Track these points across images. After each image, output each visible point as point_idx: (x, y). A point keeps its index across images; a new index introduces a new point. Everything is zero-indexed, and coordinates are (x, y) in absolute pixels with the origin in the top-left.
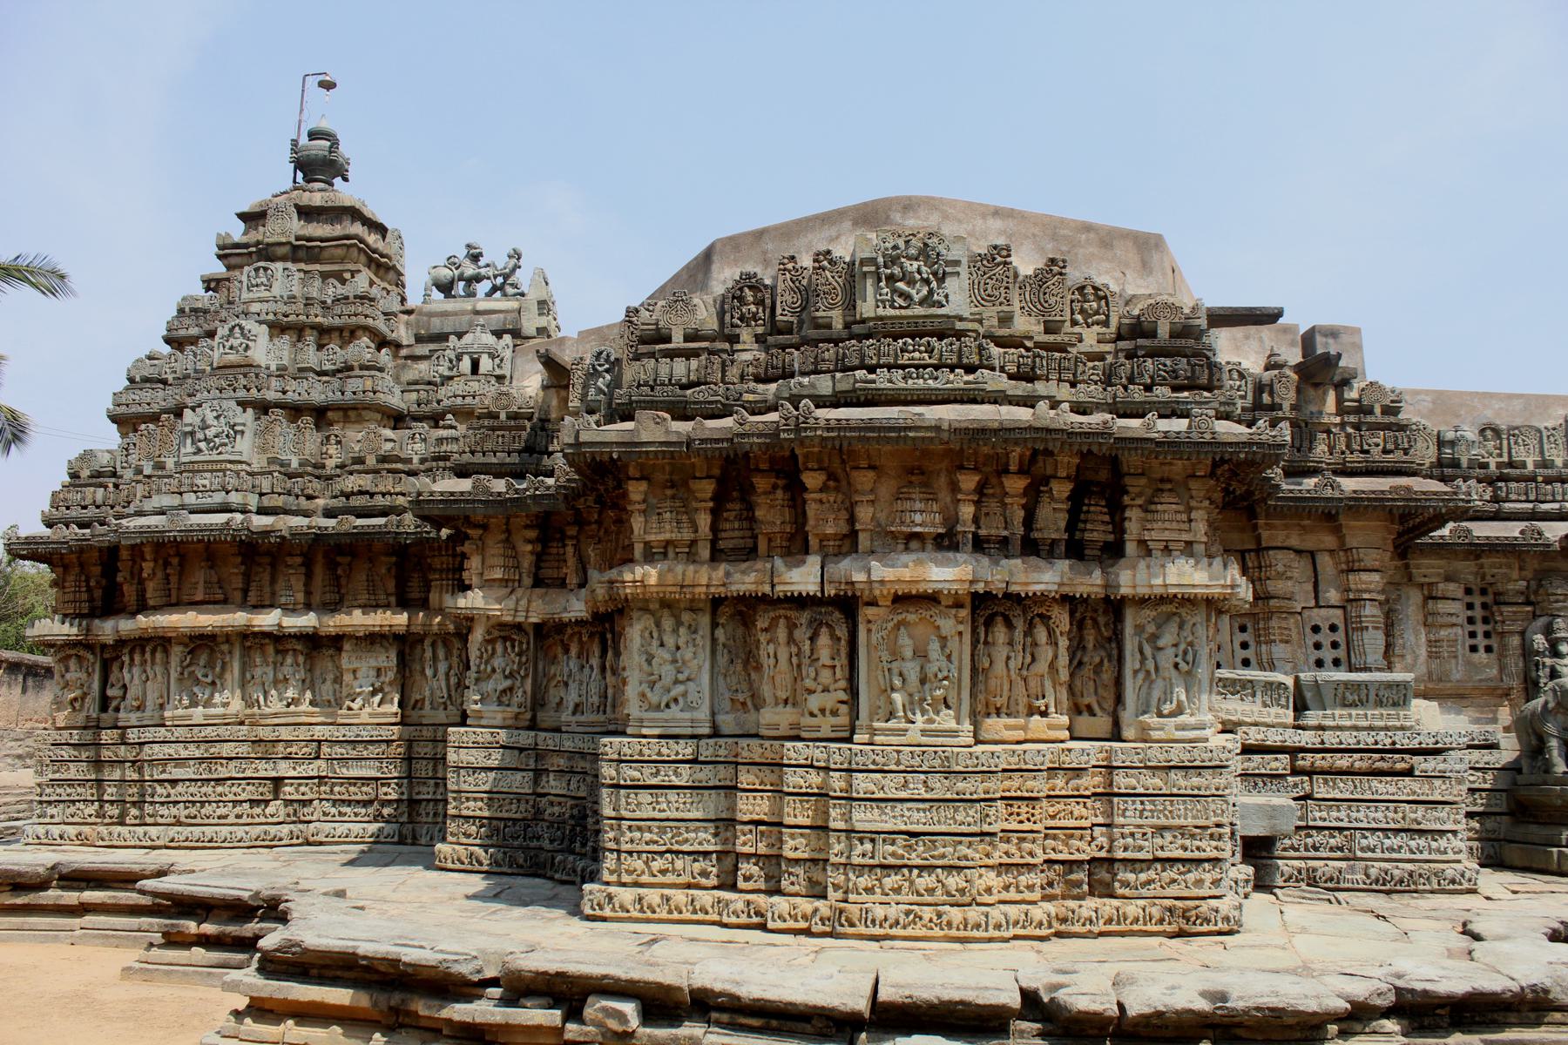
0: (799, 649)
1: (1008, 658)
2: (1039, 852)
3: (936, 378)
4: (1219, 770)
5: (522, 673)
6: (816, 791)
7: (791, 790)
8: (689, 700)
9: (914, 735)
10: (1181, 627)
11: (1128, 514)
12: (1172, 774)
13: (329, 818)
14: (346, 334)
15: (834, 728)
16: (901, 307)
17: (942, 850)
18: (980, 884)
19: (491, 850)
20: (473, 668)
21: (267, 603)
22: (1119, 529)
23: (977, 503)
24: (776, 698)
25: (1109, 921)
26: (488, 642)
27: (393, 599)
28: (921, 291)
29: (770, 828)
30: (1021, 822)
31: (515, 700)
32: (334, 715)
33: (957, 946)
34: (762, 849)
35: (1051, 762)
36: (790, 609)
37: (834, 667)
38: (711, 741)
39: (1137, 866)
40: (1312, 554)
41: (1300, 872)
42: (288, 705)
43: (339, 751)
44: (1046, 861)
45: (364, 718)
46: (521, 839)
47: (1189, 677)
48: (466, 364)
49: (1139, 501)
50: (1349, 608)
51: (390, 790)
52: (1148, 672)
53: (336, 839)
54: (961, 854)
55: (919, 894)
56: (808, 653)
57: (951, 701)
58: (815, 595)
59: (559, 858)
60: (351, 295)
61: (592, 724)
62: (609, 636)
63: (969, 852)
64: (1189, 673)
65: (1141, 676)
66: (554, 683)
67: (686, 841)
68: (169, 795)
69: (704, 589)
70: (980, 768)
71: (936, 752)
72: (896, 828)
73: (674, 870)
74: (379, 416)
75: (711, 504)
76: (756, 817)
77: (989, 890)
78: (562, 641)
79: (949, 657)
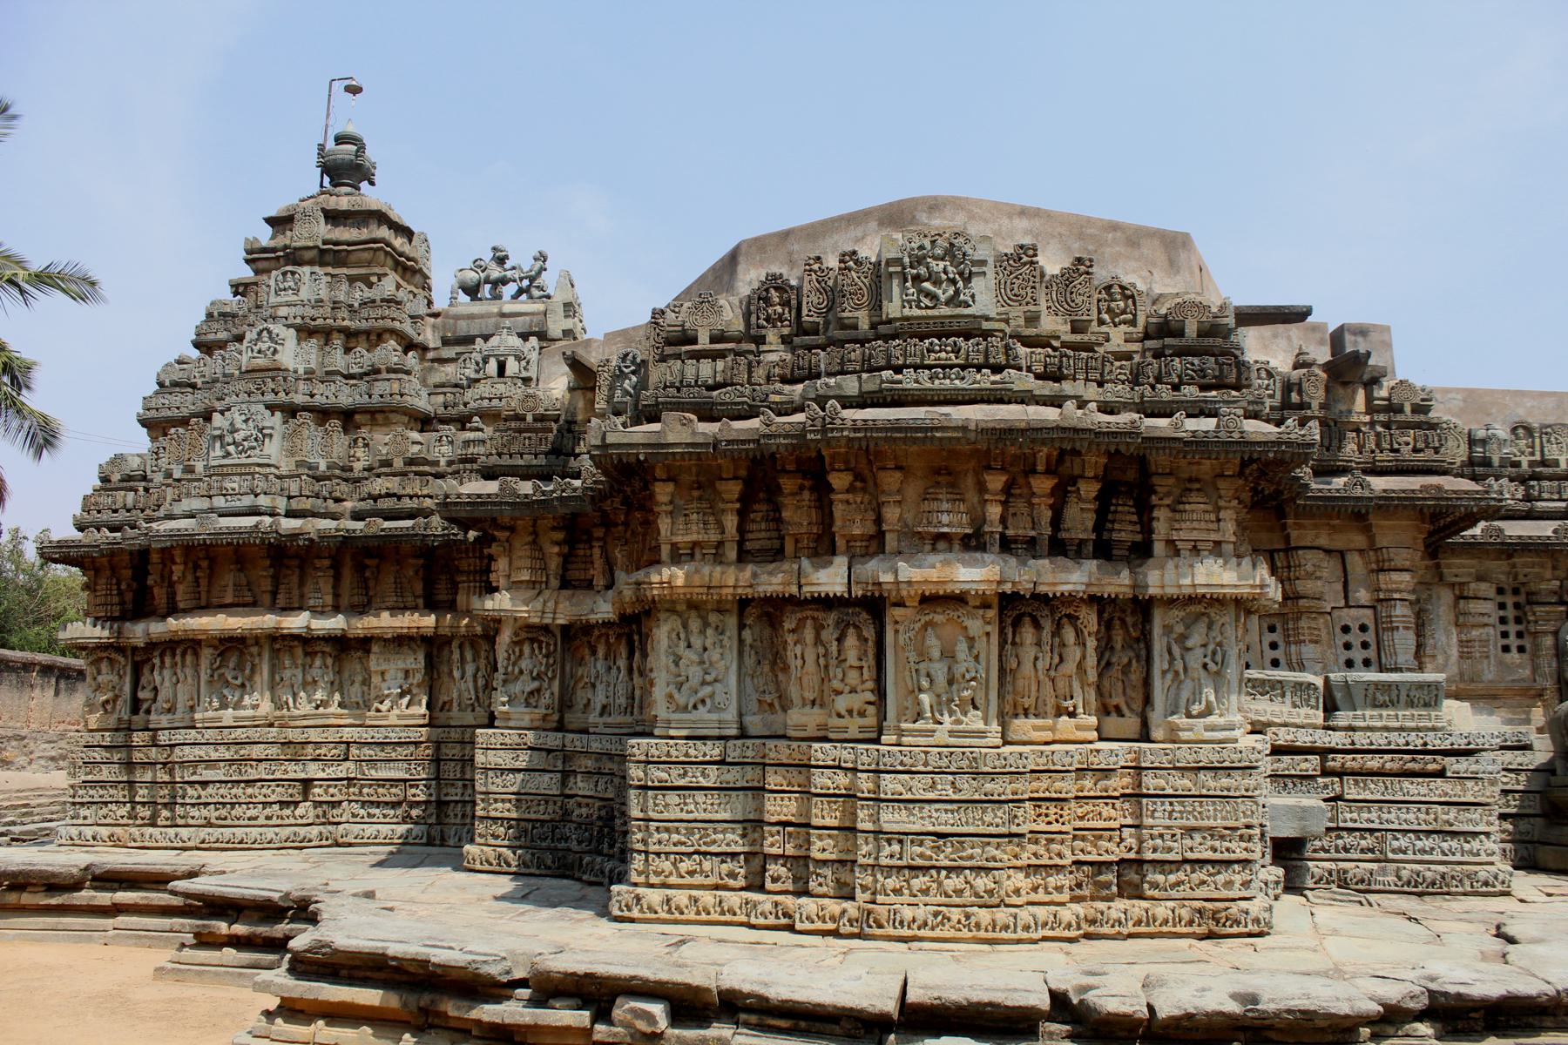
0: (827, 650)
1: (1036, 659)
2: (1068, 853)
3: (963, 378)
4: (1249, 771)
5: (550, 674)
6: (844, 792)
7: (819, 791)
9: (942, 736)
10: (1210, 627)
11: (1156, 514)
12: (1201, 775)
13: (358, 820)
14: (373, 337)
15: (862, 729)
16: (927, 307)
17: (970, 851)
18: (1009, 885)
19: (519, 852)
20: (501, 670)
22: (1147, 530)
23: (1005, 504)
24: (804, 699)
25: (1138, 923)
26: (516, 643)
27: (421, 601)
28: (948, 292)
29: (798, 829)
30: (1049, 823)
31: (543, 702)
32: (363, 716)
33: (986, 947)
34: (790, 850)
35: (1080, 763)
38: (739, 742)
39: (1167, 867)
40: (1342, 554)
41: (1330, 874)
42: (317, 707)
43: (367, 752)
44: (1074, 863)
45: (393, 720)
46: (549, 841)
47: (1218, 677)
48: (492, 367)
49: (1167, 501)
50: (1379, 608)
51: (418, 792)
52: (1177, 673)
53: (365, 840)
54: (989, 855)
55: (947, 895)
56: (835, 654)
57: (978, 702)
58: (842, 596)
59: (587, 859)
60: (378, 298)
61: (619, 725)
62: (636, 637)
63: (998, 853)
64: (1218, 673)
65: (1169, 676)
66: (581, 685)
67: (714, 842)
68: (199, 797)
70: (1008, 769)
71: (963, 753)
72: (924, 829)
73: (702, 872)
74: (406, 419)
75: (738, 505)
76: (784, 818)
77: (1017, 892)
78: (589, 642)
79: (977, 658)
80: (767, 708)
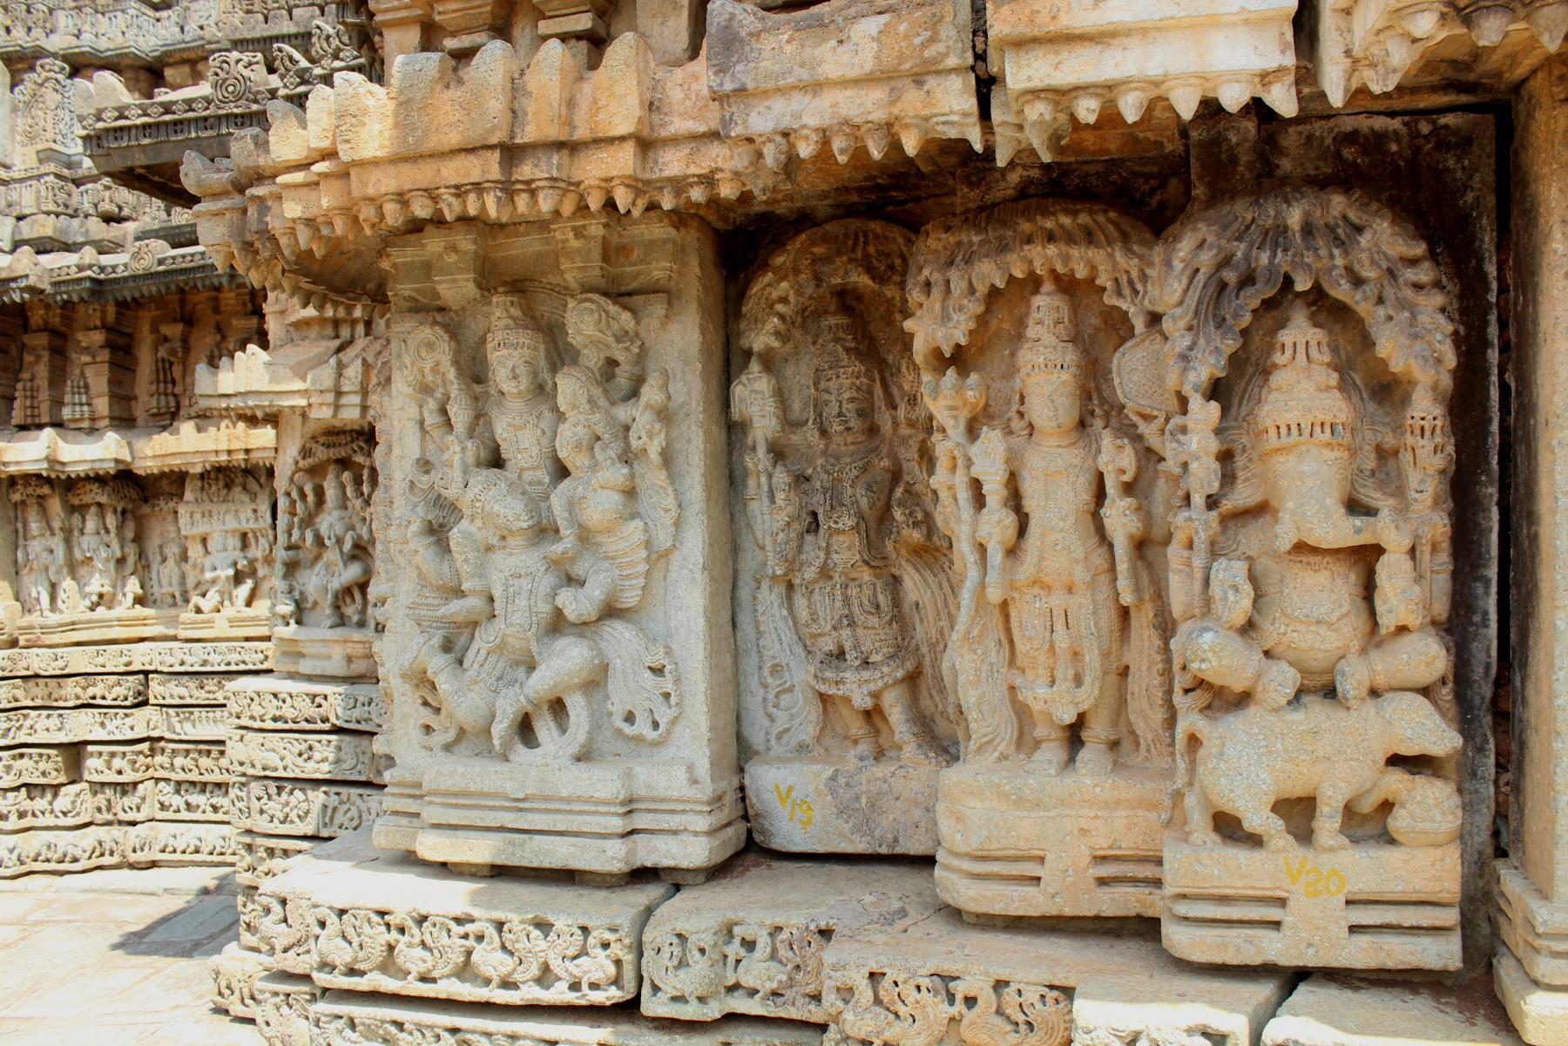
0: (1149, 456)
8: (617, 709)
13: (170, 815)
21: (46, 419)
24: (1022, 713)
32: (174, 621)
36: (1089, 238)
37: (1366, 557)
45: (221, 627)
53: (178, 856)
56: (1204, 476)
58: (1256, 114)
69: (623, 161)
80: (857, 727)
